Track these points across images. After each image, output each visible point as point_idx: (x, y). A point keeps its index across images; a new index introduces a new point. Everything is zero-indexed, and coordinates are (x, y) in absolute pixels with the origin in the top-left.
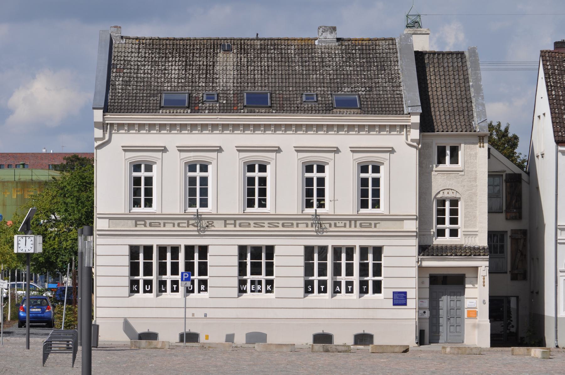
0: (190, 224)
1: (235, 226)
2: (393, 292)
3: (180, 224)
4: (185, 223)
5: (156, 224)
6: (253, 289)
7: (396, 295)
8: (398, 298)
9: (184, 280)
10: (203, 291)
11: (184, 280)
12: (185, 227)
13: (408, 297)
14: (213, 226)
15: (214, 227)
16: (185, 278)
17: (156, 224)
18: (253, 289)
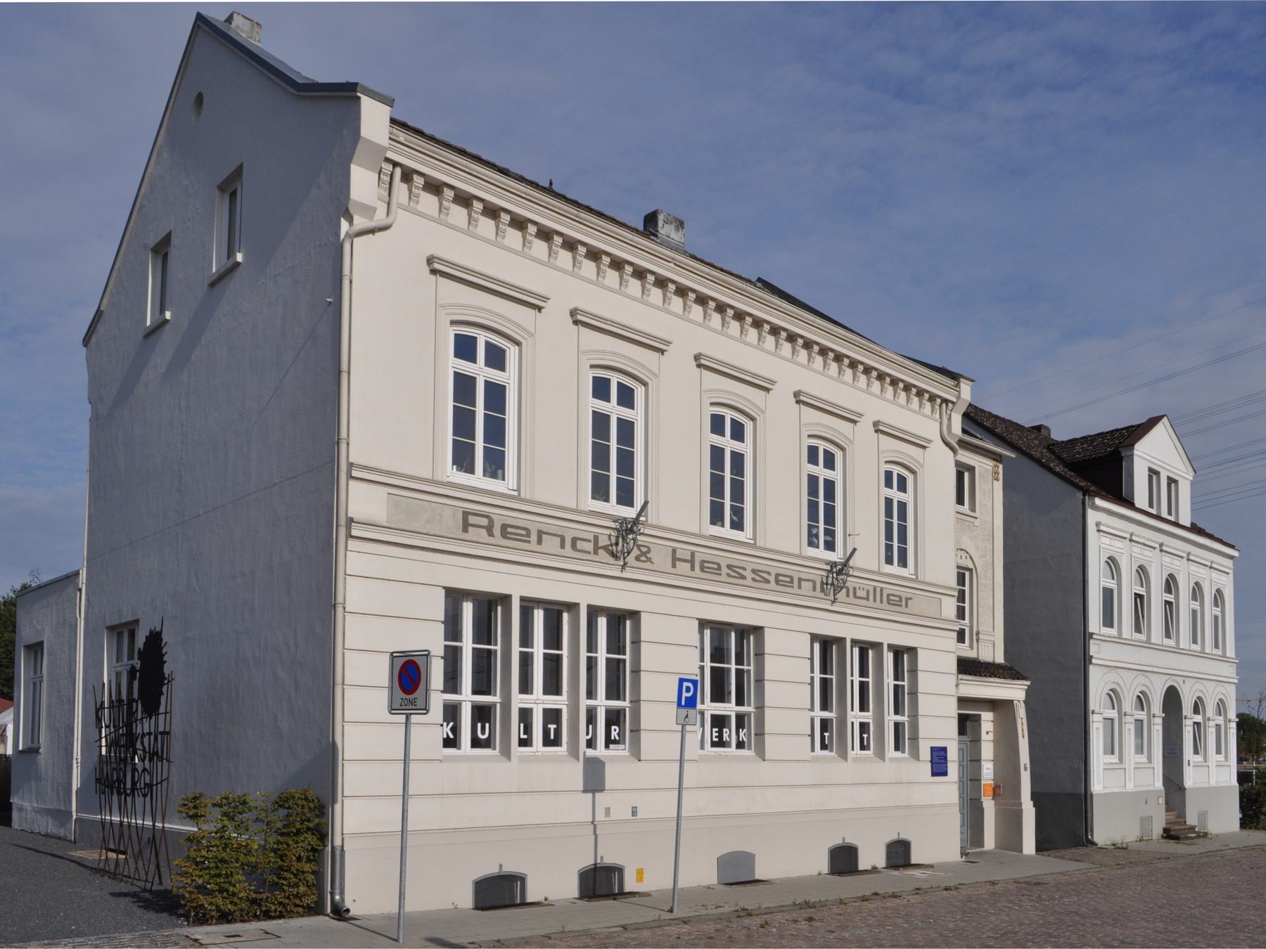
0: (600, 545)
1: (693, 568)
2: (932, 748)
3: (578, 542)
4: (590, 541)
5: (519, 531)
6: (716, 737)
7: (935, 754)
8: (938, 761)
9: (683, 704)
10: (615, 742)
11: (683, 704)
12: (590, 553)
13: (948, 759)
14: (649, 560)
15: (652, 563)
16: (686, 698)
17: (519, 531)
18: (716, 737)
